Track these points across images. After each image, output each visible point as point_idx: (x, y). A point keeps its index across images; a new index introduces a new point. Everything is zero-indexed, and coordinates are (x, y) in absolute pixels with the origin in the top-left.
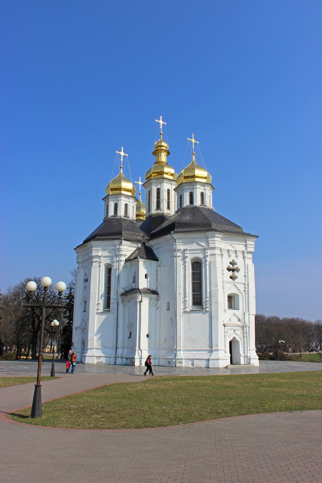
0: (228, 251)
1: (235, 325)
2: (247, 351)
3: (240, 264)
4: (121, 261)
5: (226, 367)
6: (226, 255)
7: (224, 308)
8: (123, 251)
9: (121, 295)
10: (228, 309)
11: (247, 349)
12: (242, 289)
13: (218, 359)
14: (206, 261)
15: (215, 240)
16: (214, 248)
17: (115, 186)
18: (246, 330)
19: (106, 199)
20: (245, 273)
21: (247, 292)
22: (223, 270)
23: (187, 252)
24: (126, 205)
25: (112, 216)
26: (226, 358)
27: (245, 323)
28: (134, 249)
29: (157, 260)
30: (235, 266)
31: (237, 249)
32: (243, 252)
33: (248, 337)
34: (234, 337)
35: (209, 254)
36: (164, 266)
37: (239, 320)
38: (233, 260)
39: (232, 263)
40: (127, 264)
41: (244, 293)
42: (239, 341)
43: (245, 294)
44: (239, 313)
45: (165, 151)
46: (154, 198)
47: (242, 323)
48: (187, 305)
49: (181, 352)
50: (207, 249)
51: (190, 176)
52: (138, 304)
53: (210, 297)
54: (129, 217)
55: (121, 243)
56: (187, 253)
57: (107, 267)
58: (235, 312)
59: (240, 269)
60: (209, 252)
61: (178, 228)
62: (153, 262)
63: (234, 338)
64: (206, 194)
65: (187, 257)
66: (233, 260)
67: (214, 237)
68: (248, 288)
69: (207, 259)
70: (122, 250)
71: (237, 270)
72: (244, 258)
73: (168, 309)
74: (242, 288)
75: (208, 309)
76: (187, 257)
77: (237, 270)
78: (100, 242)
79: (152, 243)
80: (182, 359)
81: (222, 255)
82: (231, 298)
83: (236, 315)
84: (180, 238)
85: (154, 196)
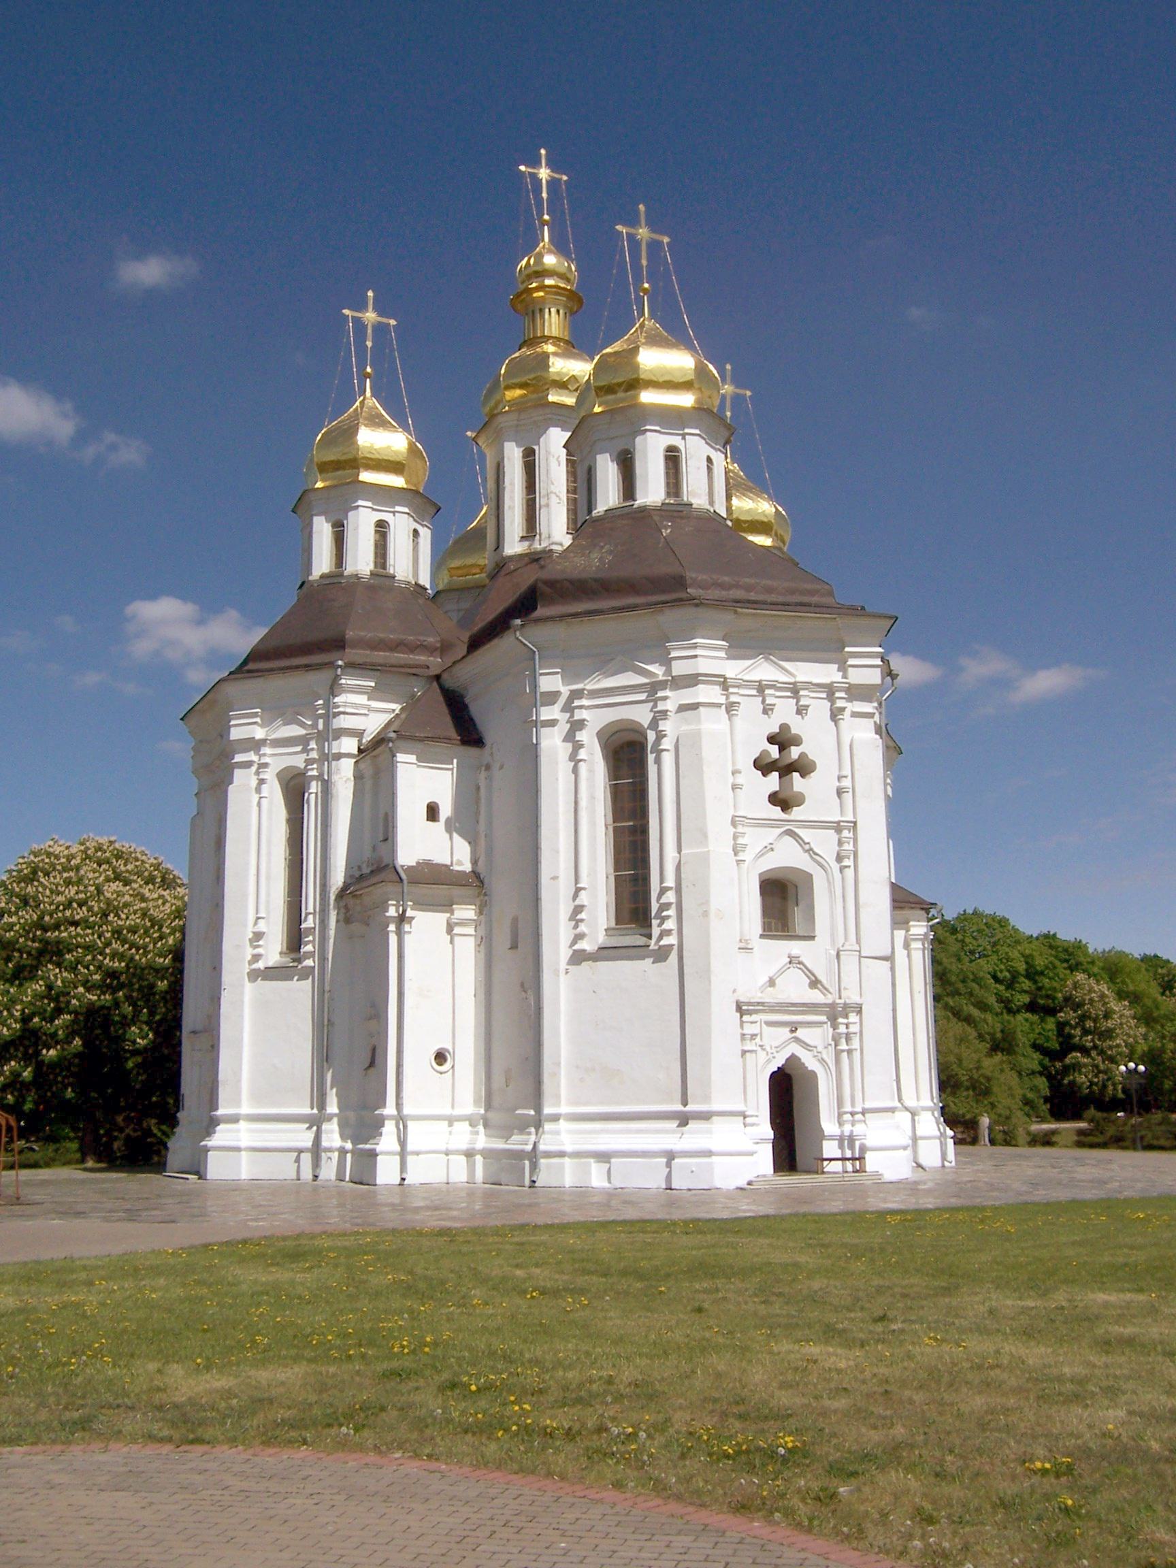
0: (761, 688)
2: (852, 1114)
4: (339, 756)
5: (749, 1183)
6: (750, 705)
7: (742, 933)
8: (344, 713)
10: (762, 936)
11: (853, 1105)
13: (709, 1153)
14: (660, 736)
15: (695, 646)
16: (692, 680)
17: (331, 456)
18: (847, 1026)
20: (840, 778)
23: (585, 702)
24: (381, 526)
25: (323, 576)
26: (750, 1147)
27: (844, 994)
30: (795, 752)
31: (799, 679)
32: (830, 690)
33: (857, 1055)
34: (793, 1059)
35: (670, 706)
36: (501, 767)
37: (815, 983)
38: (784, 727)
39: (782, 739)
40: (362, 766)
42: (813, 1076)
43: (842, 869)
46: (513, 491)
47: (829, 996)
48: (583, 928)
49: (563, 1125)
50: (662, 685)
51: (619, 385)
52: (392, 927)
53: (678, 889)
55: (334, 689)
56: (581, 707)
57: (292, 784)
58: (795, 947)
59: (814, 762)
60: (672, 699)
61: (551, 601)
63: (793, 1059)
64: (691, 451)
66: (784, 727)
69: (662, 726)
70: (341, 709)
71: (803, 767)
72: (835, 714)
73: (514, 946)
75: (671, 940)
77: (803, 767)
80: (562, 1154)
81: (730, 707)
83: (800, 963)
85: (512, 484)
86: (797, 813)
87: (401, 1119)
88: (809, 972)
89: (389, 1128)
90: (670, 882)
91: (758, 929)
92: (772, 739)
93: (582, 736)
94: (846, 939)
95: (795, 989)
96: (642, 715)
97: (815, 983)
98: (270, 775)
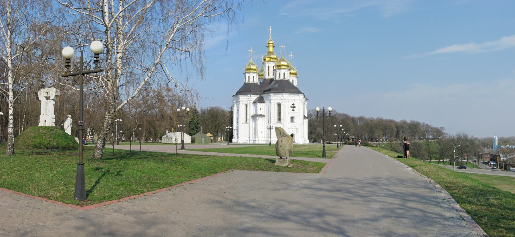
1: (293, 129)
9: (251, 117)
16: (285, 99)
19: (245, 73)
24: (253, 76)
25: (247, 82)
28: (256, 98)
29: (264, 103)
35: (283, 101)
39: (293, 105)
41: (297, 116)
42: (294, 135)
45: (272, 46)
55: (251, 96)
60: (283, 101)
62: (263, 104)
65: (275, 103)
67: (285, 95)
71: (294, 107)
76: (275, 103)
77: (294, 107)
78: (242, 96)
79: (263, 95)
81: (288, 102)
82: (292, 118)
84: (272, 95)
86: (294, 111)
87: (258, 138)
89: (257, 138)
90: (283, 117)
91: (290, 122)
92: (292, 105)
93: (275, 104)
95: (293, 127)
96: (280, 102)
97: (295, 126)
98: (244, 104)
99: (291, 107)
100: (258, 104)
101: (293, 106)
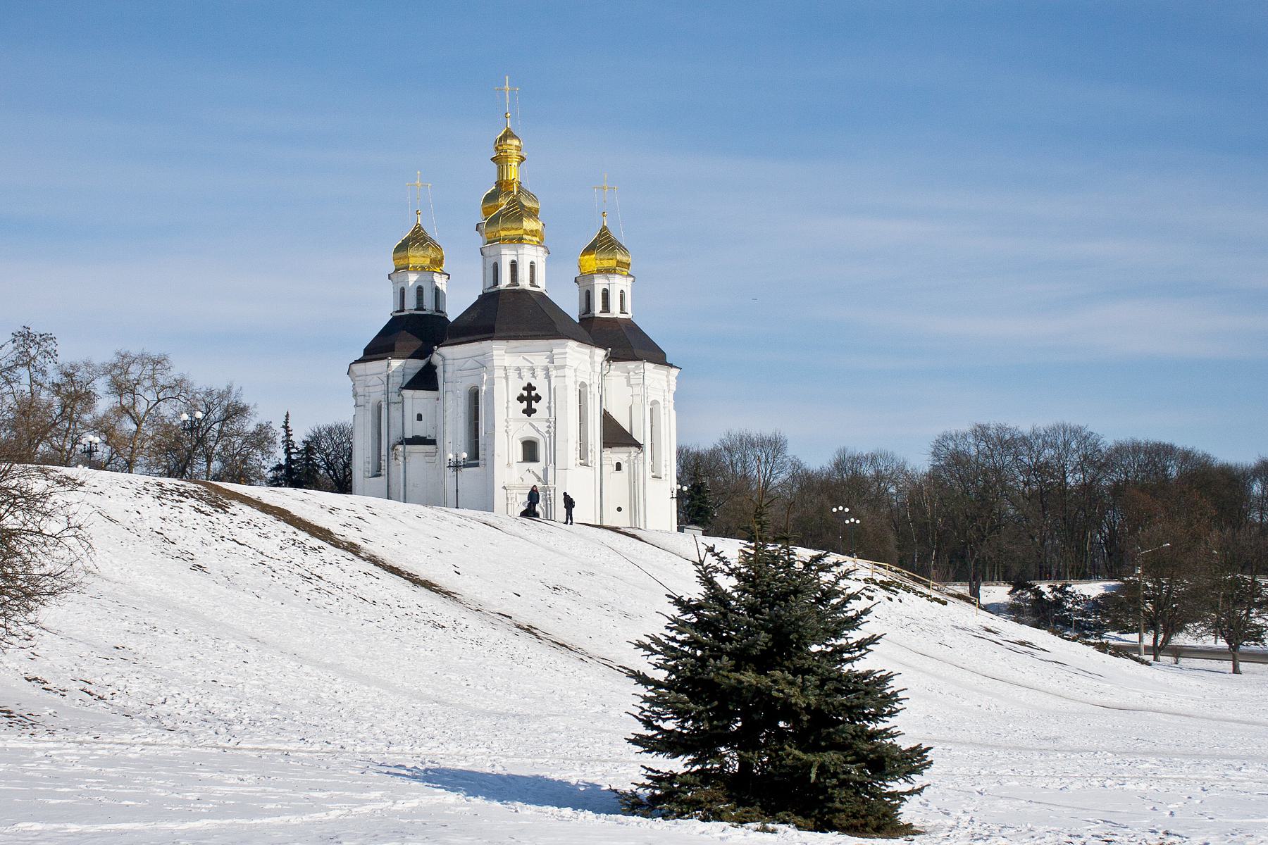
0: (519, 369)
3: (541, 390)
12: (543, 428)
20: (549, 403)
21: (552, 434)
22: (508, 402)
30: (533, 393)
38: (529, 385)
39: (529, 388)
41: (547, 435)
43: (550, 437)
44: (537, 467)
54: (425, 310)
58: (532, 466)
66: (529, 385)
68: (555, 428)
72: (548, 377)
74: (543, 427)
81: (507, 378)
88: (537, 476)
92: (524, 389)
94: (550, 463)
99: (521, 399)
100: (408, 393)
101: (529, 398)
